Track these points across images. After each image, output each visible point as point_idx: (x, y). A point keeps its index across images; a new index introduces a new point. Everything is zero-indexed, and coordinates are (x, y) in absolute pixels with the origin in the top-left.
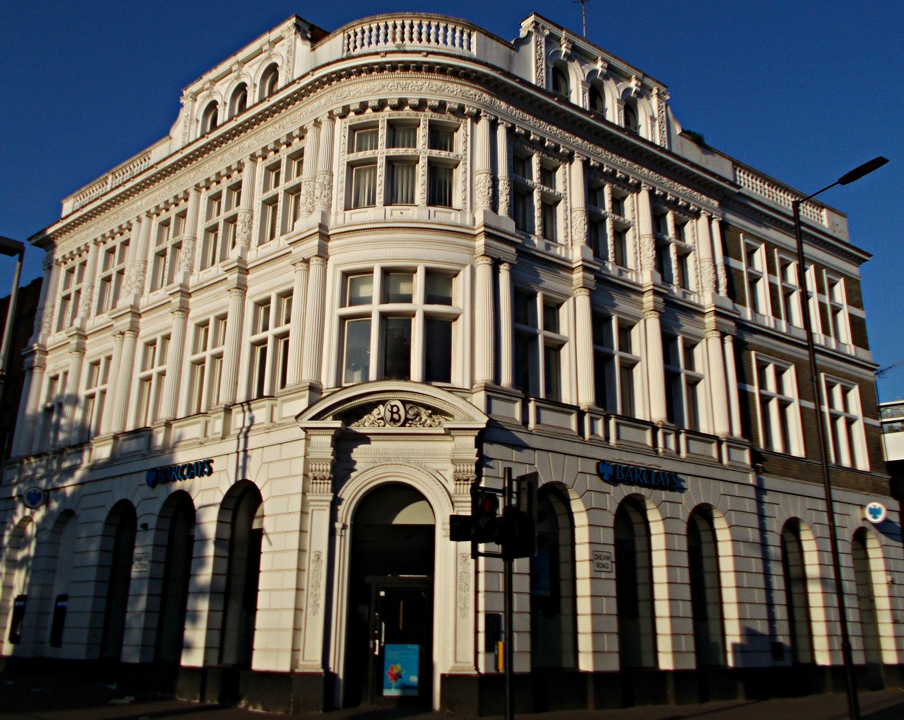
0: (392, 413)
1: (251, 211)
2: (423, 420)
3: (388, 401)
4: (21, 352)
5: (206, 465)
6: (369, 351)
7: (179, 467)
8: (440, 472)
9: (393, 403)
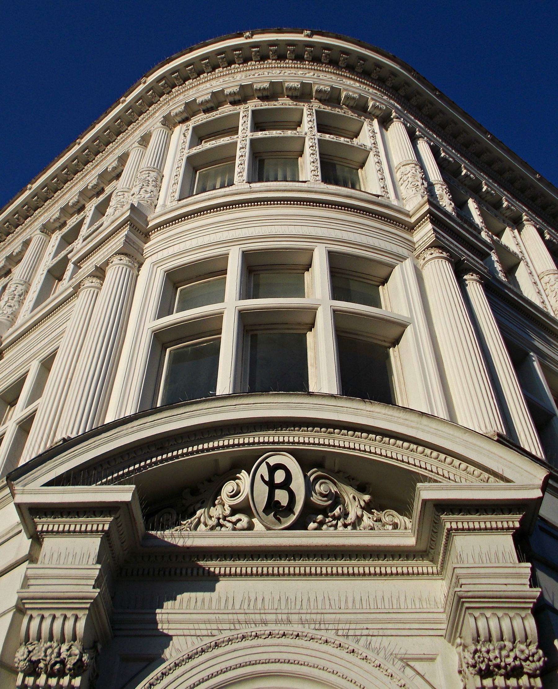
0: (272, 486)
1: (28, 284)
2: (351, 518)
8: (417, 665)
9: (272, 461)
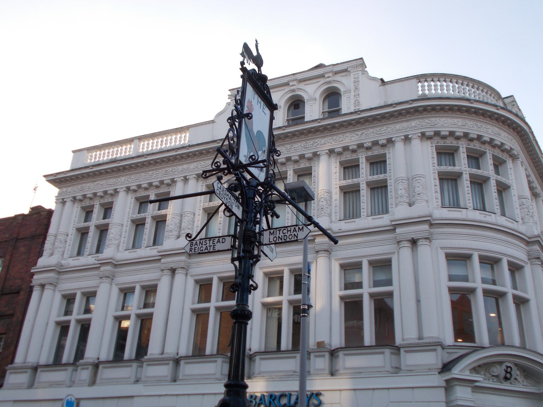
0: (506, 372)
1: (329, 192)
3: (506, 362)
4: (31, 269)
5: (314, 395)
6: (471, 318)
7: (276, 396)
9: (509, 365)
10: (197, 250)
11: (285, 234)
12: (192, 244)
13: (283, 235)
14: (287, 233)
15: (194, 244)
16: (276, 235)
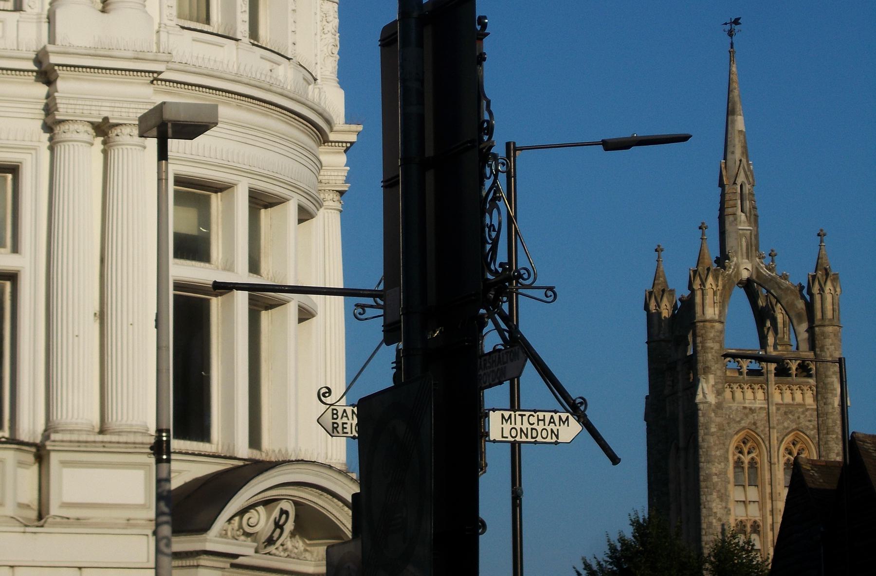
0: (278, 525)
10: (348, 430)
11: (533, 427)
12: (336, 414)
13: (530, 427)
14: (538, 425)
15: (340, 416)
16: (515, 424)
